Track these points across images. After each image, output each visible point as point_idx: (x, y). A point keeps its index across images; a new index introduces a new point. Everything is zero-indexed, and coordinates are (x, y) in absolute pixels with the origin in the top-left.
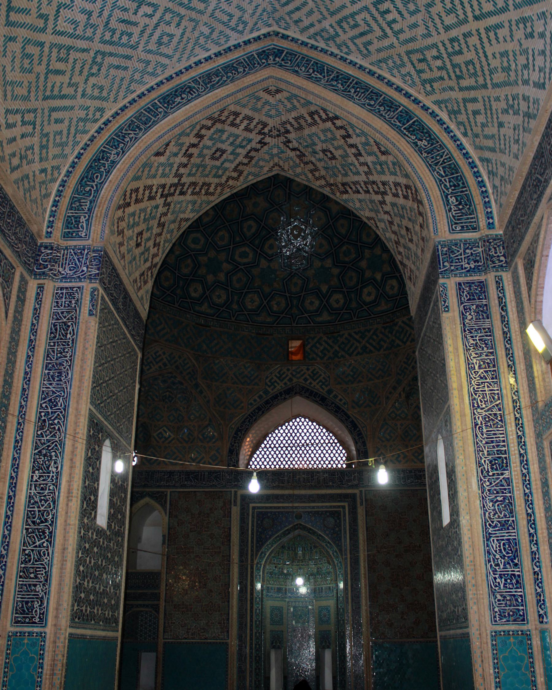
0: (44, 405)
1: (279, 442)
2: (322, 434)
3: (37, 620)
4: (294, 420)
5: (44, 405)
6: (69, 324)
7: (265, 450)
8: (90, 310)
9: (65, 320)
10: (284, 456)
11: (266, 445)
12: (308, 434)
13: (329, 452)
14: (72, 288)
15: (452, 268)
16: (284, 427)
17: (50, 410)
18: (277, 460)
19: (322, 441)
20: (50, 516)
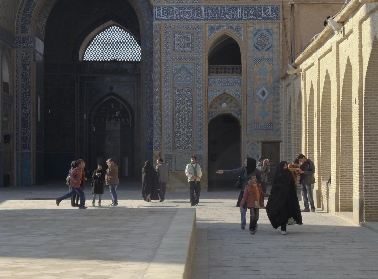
0: (23, 90)
1: (102, 41)
2: (127, 37)
3: (28, 149)
4: (110, 28)
5: (23, 90)
6: (27, 64)
7: (94, 45)
8: (33, 59)
9: (26, 62)
10: (105, 49)
11: (94, 43)
12: (119, 36)
13: (131, 47)
14: (27, 51)
15: (145, 47)
16: (105, 32)
17: (25, 91)
18: (101, 51)
19: (127, 41)
20: (29, 122)
